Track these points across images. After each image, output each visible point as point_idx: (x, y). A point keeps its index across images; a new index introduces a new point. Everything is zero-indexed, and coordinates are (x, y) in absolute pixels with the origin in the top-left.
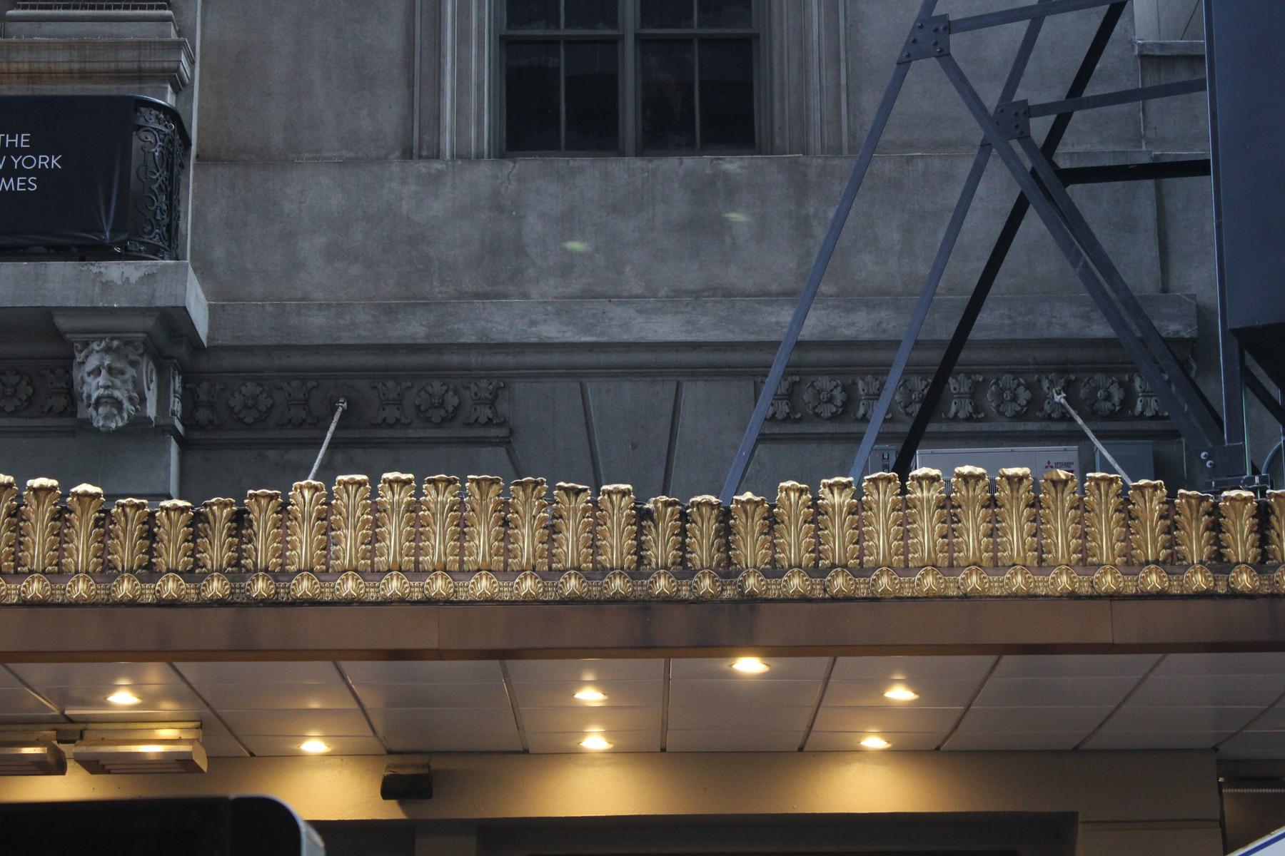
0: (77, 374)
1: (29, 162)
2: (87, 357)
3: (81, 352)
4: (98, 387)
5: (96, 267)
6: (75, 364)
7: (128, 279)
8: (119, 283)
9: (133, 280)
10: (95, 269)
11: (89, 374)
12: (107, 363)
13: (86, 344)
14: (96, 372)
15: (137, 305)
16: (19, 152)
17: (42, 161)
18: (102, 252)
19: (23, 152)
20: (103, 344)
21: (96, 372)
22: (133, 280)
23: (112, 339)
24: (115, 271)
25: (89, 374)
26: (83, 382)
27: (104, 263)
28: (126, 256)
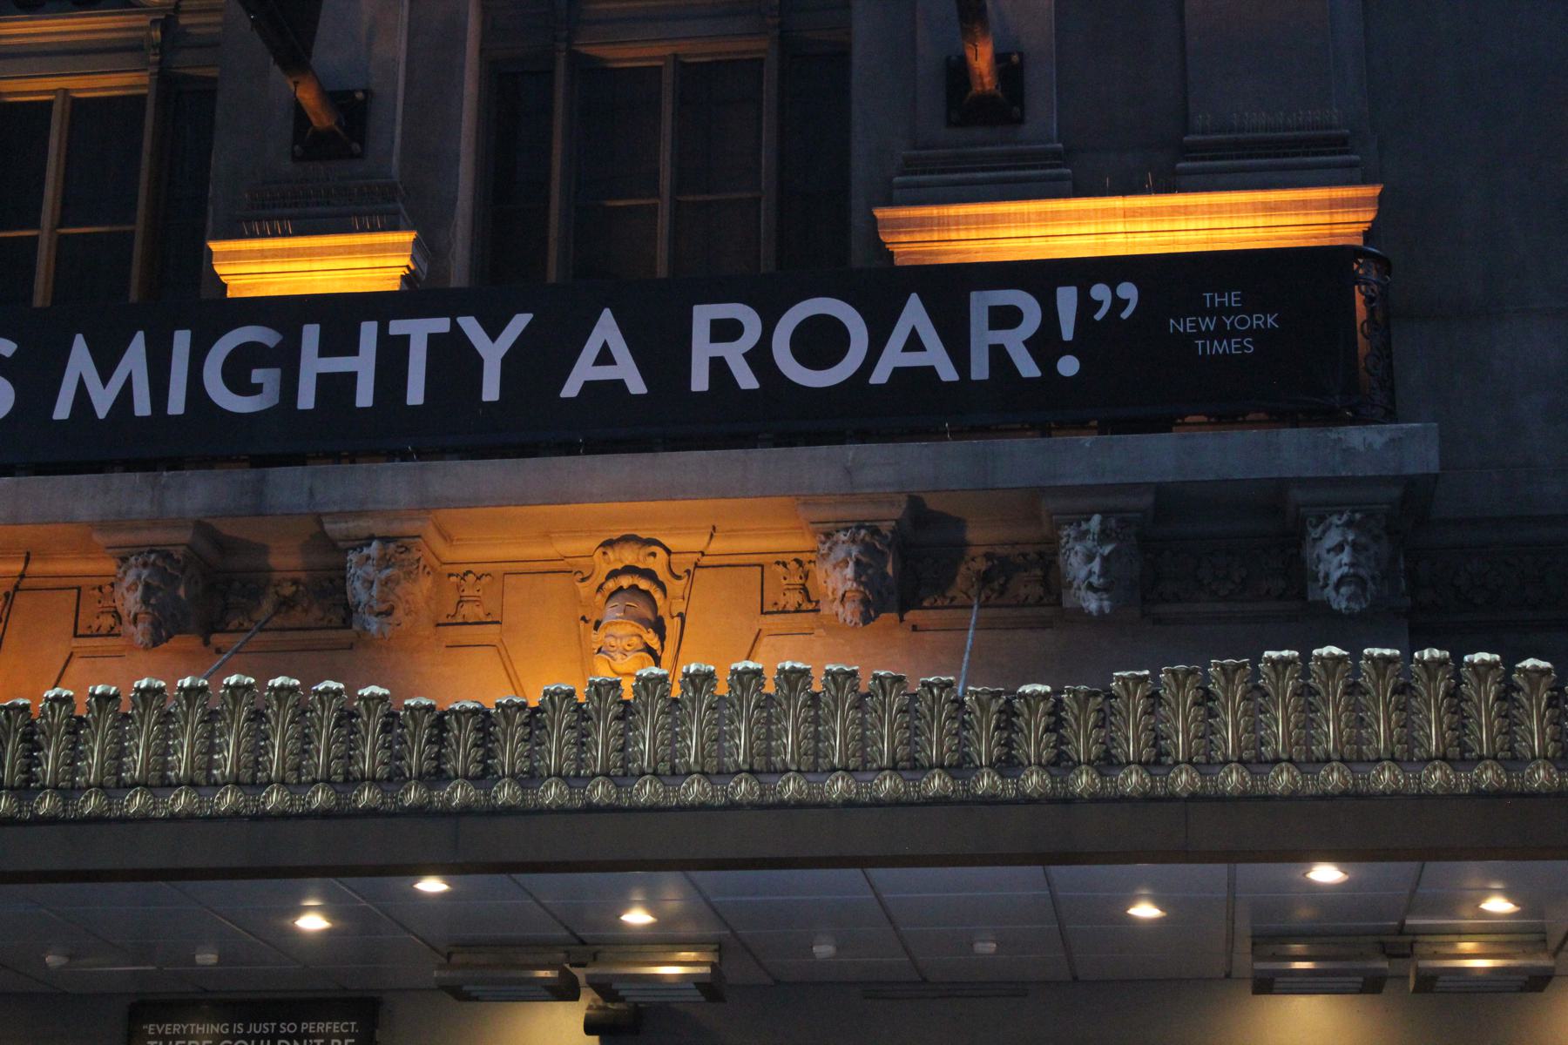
0: (1310, 553)
1: (1243, 322)
2: (1324, 532)
3: (1316, 526)
4: (1340, 566)
5: (1334, 434)
6: (1309, 539)
7: (1370, 445)
8: (1362, 449)
9: (1377, 446)
10: (1333, 436)
11: (1329, 551)
12: (1350, 538)
13: (1321, 519)
14: (1339, 548)
15: (1384, 473)
16: (1231, 311)
17: (1256, 321)
18: (1331, 417)
19: (1236, 311)
20: (1345, 517)
21: (1339, 548)
22: (1377, 446)
23: (1353, 512)
24: (1356, 436)
25: (1329, 551)
26: (1319, 559)
27: (1342, 429)
28: (1359, 420)
